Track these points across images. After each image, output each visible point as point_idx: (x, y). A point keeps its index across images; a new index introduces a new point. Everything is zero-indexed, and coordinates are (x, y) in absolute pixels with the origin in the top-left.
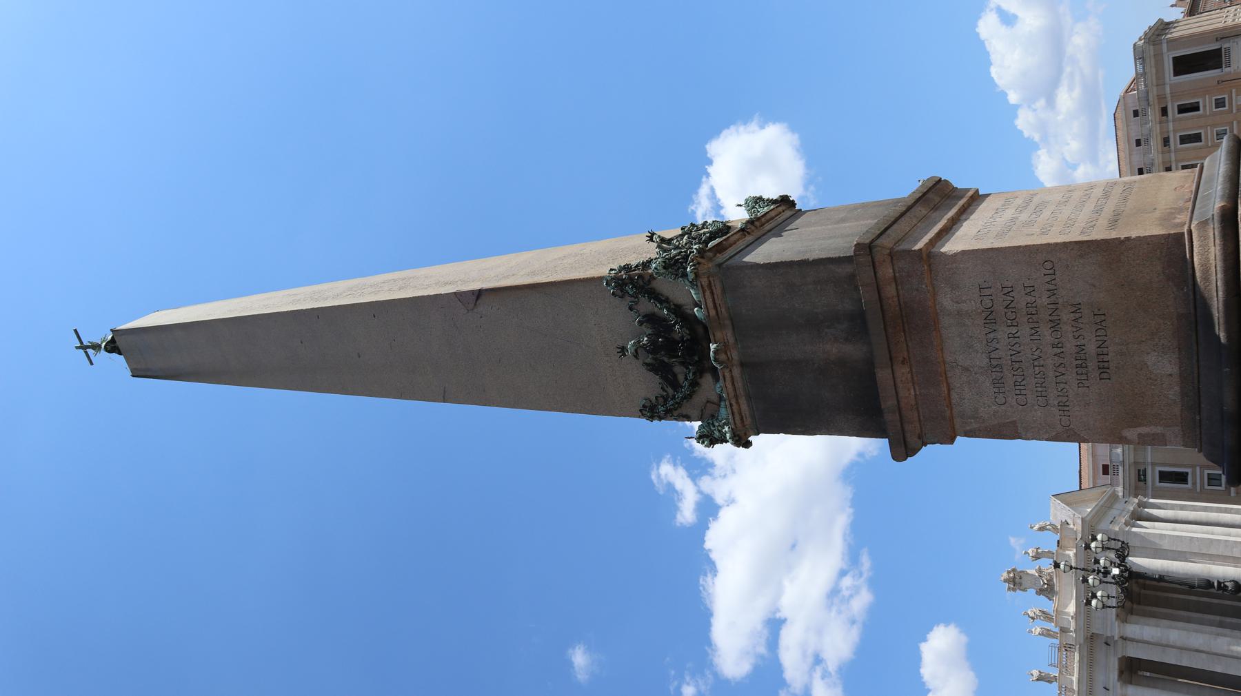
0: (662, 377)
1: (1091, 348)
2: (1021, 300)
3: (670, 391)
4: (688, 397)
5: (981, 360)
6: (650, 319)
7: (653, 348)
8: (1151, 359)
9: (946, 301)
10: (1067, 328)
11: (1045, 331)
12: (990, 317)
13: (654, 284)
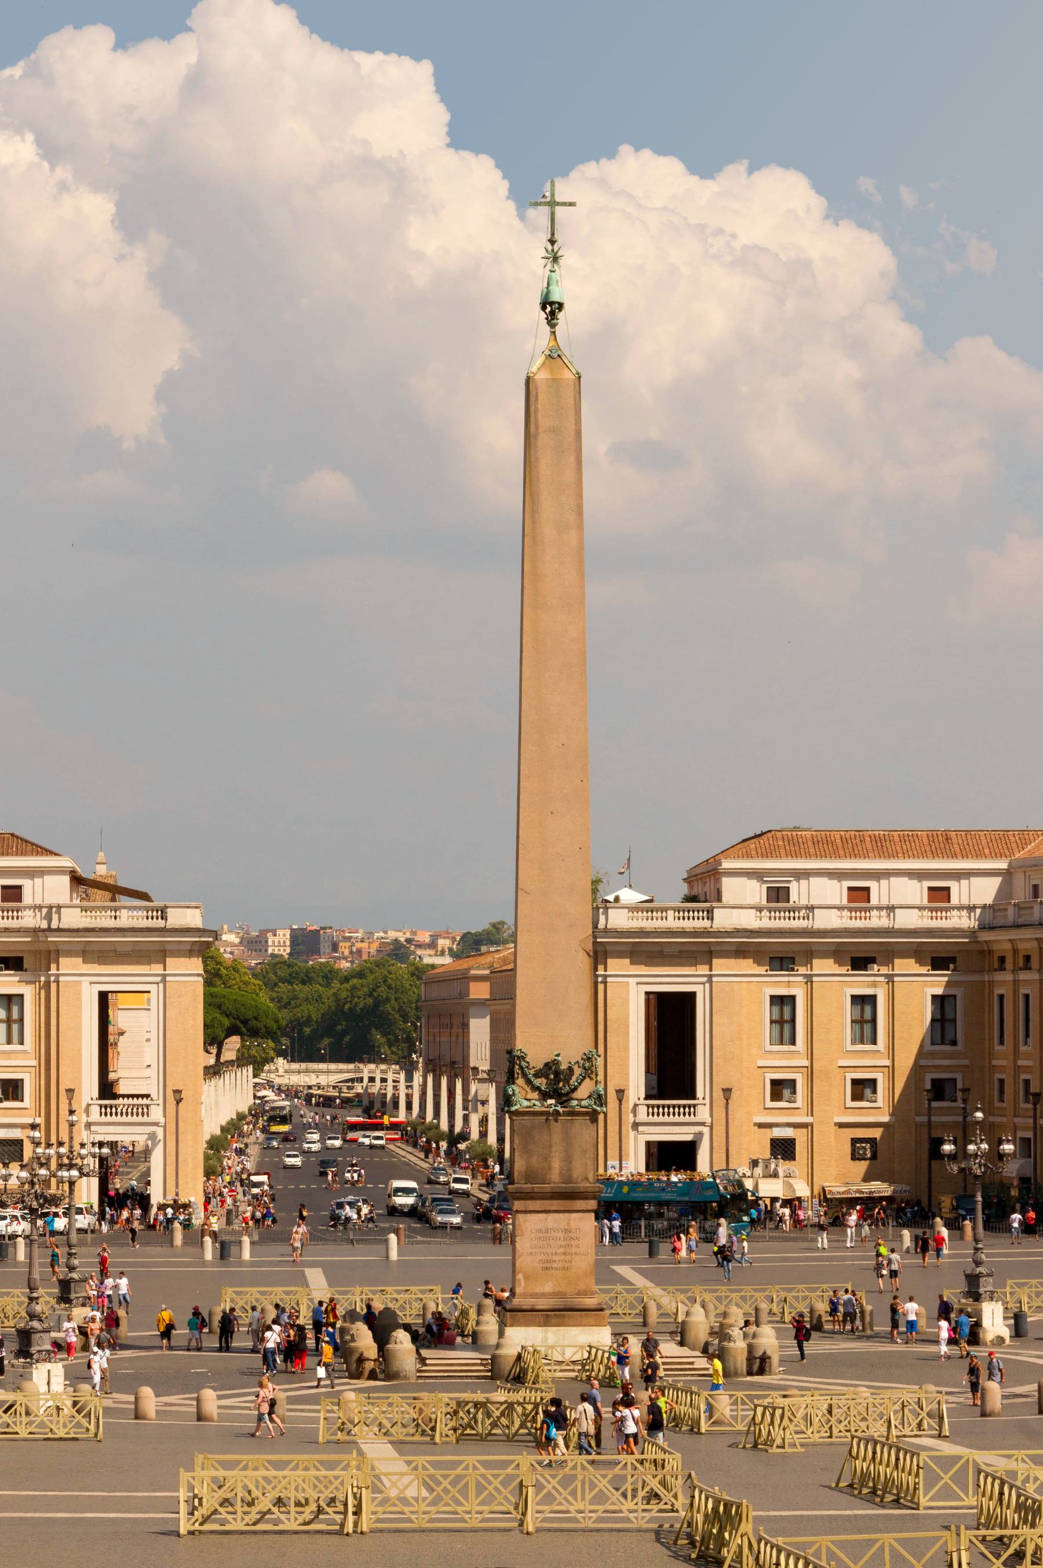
0: (541, 1070)
1: (555, 1265)
2: (574, 1243)
3: (532, 1072)
4: (529, 1082)
5: (550, 1225)
6: (571, 1070)
7: (557, 1074)
8: (550, 1284)
9: (574, 1215)
10: (563, 1257)
11: (562, 1250)
12: (568, 1231)
13: (587, 1080)
